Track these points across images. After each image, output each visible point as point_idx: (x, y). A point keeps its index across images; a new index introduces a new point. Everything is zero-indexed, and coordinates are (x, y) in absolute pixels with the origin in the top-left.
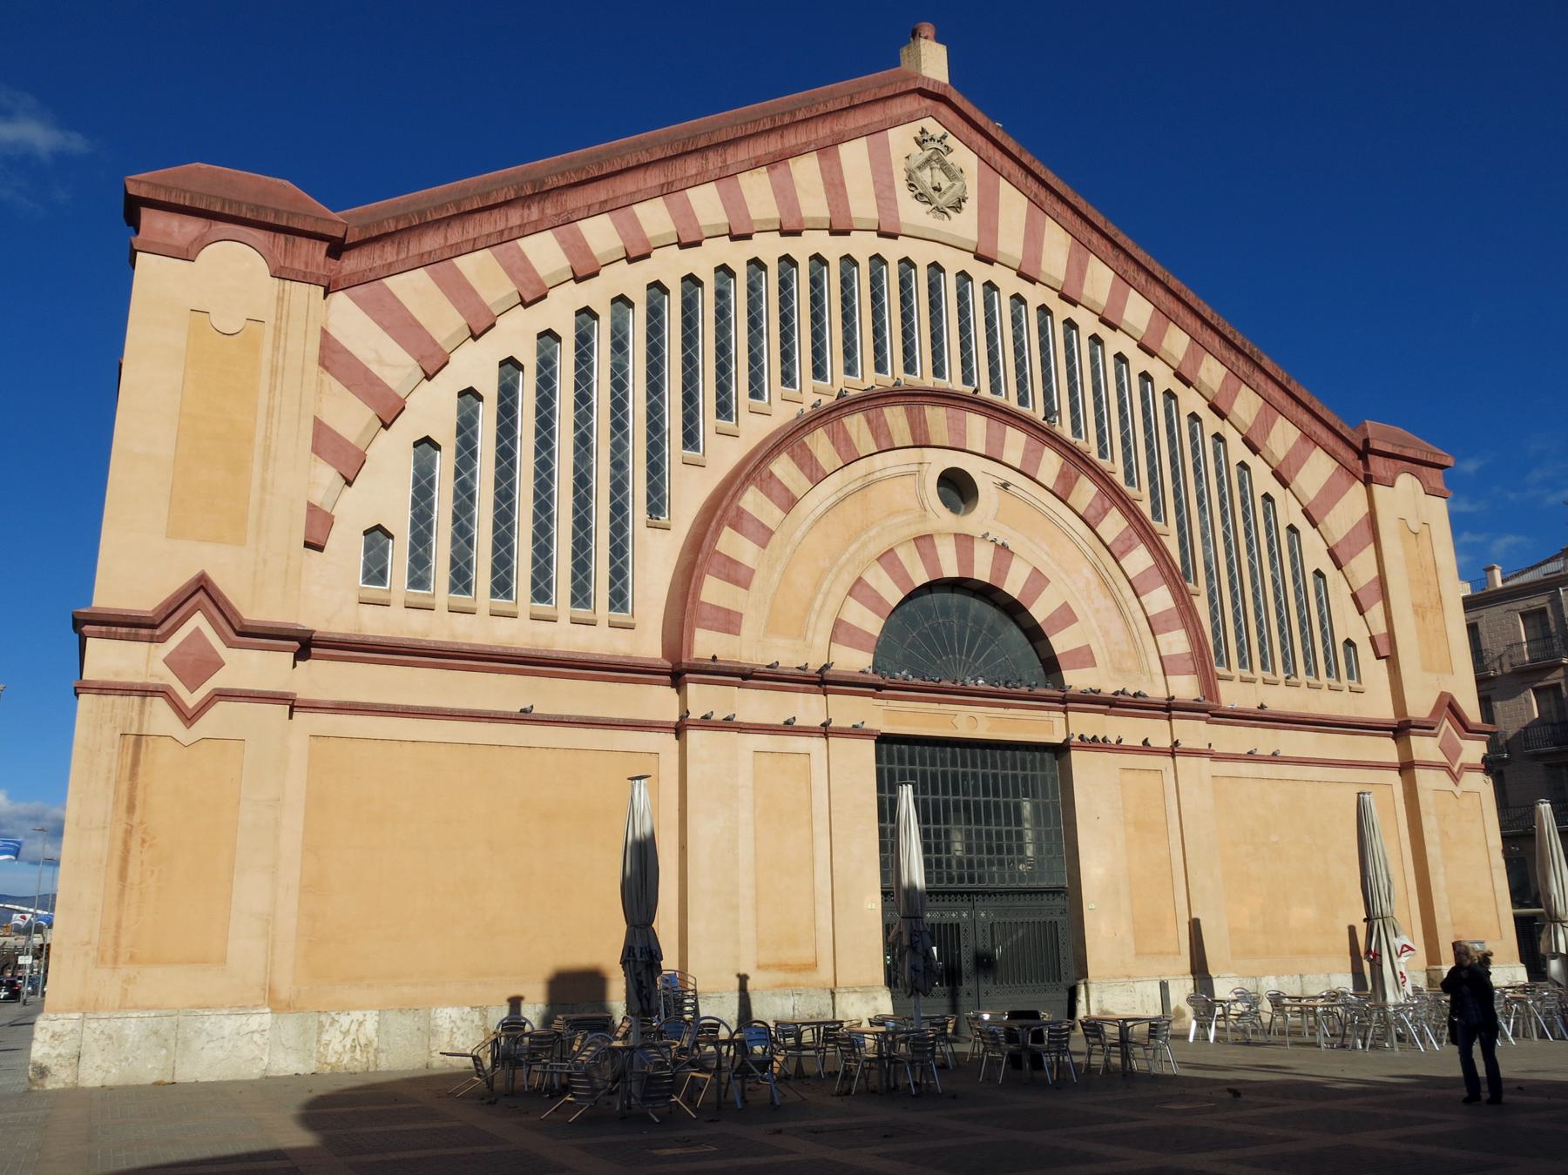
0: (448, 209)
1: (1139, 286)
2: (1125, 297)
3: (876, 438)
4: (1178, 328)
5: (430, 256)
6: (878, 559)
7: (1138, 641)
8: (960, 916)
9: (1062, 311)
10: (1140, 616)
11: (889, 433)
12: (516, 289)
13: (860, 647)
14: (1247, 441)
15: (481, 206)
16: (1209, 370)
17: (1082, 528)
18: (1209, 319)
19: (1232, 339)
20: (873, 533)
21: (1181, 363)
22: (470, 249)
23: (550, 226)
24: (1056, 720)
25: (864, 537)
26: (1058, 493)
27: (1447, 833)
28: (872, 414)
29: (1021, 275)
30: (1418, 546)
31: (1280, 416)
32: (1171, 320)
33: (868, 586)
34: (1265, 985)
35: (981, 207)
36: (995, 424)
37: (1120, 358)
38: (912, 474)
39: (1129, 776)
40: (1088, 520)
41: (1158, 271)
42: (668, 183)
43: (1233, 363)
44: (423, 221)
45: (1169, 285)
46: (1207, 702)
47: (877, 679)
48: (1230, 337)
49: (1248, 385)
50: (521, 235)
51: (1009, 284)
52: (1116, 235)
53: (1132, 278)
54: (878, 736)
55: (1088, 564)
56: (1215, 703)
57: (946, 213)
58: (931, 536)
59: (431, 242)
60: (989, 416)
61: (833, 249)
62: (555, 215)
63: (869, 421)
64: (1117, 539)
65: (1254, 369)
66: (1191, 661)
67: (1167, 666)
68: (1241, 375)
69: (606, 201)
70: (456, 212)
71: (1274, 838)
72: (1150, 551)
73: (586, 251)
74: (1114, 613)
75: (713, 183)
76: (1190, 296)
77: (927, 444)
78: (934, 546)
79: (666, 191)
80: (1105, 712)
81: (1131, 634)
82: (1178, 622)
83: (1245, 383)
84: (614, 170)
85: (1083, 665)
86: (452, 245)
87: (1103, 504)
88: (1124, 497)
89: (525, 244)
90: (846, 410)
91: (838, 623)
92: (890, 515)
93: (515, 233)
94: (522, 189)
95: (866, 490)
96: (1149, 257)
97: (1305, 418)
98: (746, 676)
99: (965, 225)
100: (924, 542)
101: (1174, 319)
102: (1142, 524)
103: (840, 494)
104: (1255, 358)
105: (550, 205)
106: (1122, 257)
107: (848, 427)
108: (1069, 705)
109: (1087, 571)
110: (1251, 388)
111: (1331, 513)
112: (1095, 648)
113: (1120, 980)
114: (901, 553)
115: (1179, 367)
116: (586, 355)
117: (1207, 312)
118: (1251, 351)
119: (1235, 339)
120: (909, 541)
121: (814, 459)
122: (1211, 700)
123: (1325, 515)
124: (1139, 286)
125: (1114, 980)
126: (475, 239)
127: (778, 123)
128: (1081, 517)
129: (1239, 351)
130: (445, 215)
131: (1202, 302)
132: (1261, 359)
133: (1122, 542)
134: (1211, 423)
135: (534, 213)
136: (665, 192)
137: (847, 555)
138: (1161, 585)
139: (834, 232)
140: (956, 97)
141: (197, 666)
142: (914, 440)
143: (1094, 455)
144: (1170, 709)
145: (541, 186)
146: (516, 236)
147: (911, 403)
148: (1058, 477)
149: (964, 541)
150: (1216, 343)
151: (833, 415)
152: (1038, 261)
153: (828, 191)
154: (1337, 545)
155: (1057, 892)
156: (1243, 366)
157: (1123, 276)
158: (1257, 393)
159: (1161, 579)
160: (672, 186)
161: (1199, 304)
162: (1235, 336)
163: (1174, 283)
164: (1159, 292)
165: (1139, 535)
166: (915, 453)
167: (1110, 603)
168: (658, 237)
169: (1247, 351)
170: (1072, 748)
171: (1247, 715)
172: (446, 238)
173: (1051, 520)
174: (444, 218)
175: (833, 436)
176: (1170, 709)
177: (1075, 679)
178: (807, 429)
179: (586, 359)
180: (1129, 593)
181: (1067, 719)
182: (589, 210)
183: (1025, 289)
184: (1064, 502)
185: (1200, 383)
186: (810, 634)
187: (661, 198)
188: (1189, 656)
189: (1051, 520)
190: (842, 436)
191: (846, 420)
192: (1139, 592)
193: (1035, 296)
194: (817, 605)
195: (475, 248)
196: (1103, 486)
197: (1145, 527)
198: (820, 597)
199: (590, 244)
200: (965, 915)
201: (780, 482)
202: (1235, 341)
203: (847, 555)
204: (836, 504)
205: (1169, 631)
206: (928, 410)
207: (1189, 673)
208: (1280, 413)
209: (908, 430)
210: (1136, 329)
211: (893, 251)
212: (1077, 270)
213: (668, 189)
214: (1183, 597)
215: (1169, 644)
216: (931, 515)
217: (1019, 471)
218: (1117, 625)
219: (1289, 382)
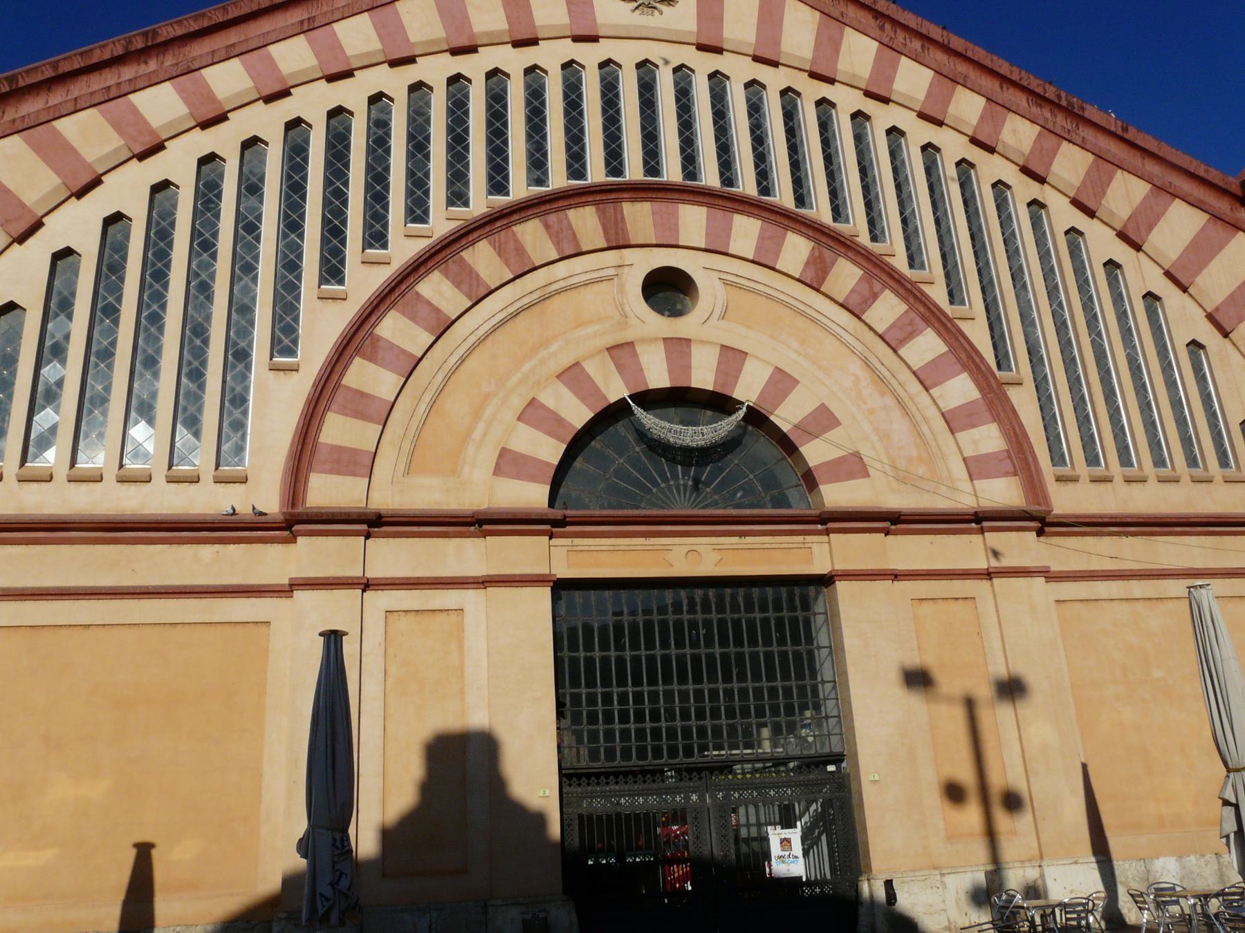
0: (43, 72)
1: (910, 51)
2: (895, 67)
3: (557, 244)
4: (968, 92)
5: (23, 121)
6: (558, 377)
7: (932, 443)
8: (687, 798)
9: (811, 91)
10: (932, 412)
11: (574, 234)
12: (123, 142)
13: (533, 479)
14: (1076, 203)
15: (83, 65)
16: (1014, 131)
17: (844, 317)
18: (1009, 76)
19: (1042, 93)
20: (554, 347)
21: (976, 128)
22: (72, 109)
23: (166, 78)
24: (816, 548)
25: (543, 354)
26: (808, 281)
28: (552, 218)
29: (756, 59)
31: (1119, 171)
32: (958, 83)
33: (543, 407)
34: (1159, 869)
36: (719, 214)
37: (894, 133)
39: (927, 608)
40: (850, 308)
41: (935, 32)
42: (309, 19)
43: (1046, 119)
44: (14, 87)
45: (951, 46)
46: (1033, 508)
47: (557, 513)
48: (1039, 90)
49: (1070, 141)
50: (133, 89)
51: (739, 70)
53: (900, 45)
54: (554, 582)
55: (856, 358)
56: (1043, 508)
57: (655, 8)
58: (631, 344)
59: (31, 107)
60: (709, 205)
61: (514, 61)
62: (173, 65)
63: (547, 227)
64: (892, 326)
65: (1077, 125)
67: (977, 468)
68: (1058, 131)
69: (233, 45)
70: (53, 75)
71: (1158, 674)
72: (940, 335)
73: (210, 95)
74: (896, 413)
75: (366, 13)
76: (979, 54)
77: (626, 243)
78: (635, 355)
79: (306, 28)
80: (887, 533)
81: (920, 435)
82: (987, 415)
83: (1066, 139)
84: (242, 13)
85: (850, 476)
86: (50, 107)
87: (871, 288)
88: (897, 276)
89: (139, 99)
90: (516, 217)
91: (504, 452)
92: (579, 325)
93: (125, 88)
95: (548, 301)
96: (920, 19)
97: (1152, 168)
100: (622, 353)
101: (961, 81)
102: (925, 305)
103: (511, 310)
104: (1076, 111)
105: (170, 58)
106: (888, 26)
107: (519, 235)
108: (831, 525)
109: (856, 367)
110: (1074, 144)
111: (1205, 272)
112: (866, 453)
113: (917, 874)
114: (591, 368)
115: (975, 132)
116: (213, 202)
117: (1004, 67)
118: (1069, 103)
119: (1045, 93)
120: (601, 351)
121: (474, 275)
122: (1039, 504)
123: (1196, 276)
124: (910, 51)
125: (912, 874)
126: (76, 99)
128: (842, 305)
129: (1055, 105)
130: (40, 77)
131: (995, 58)
132: (1083, 109)
133: (901, 329)
134: (1023, 190)
135: (152, 65)
136: (306, 28)
137: (519, 375)
138: (959, 374)
139: (517, 44)
142: (607, 240)
143: (864, 239)
144: (979, 520)
145: (153, 38)
146: (126, 91)
148: (807, 263)
149: (678, 348)
150: (1021, 100)
151: (498, 224)
152: (777, 43)
154: (1217, 309)
155: (837, 759)
156: (1061, 122)
157: (890, 45)
158: (1083, 148)
159: (958, 367)
160: (314, 22)
161: (992, 61)
163: (957, 43)
164: (939, 56)
165: (924, 319)
166: (612, 257)
167: (889, 401)
168: (292, 75)
169: (1064, 103)
170: (836, 578)
171: (1100, 520)
172: (47, 102)
173: (802, 314)
175: (500, 247)
176: (979, 520)
177: (835, 495)
178: (464, 242)
179: (212, 206)
180: (914, 386)
181: (829, 543)
182: (213, 56)
183: (763, 73)
184: (818, 290)
185: (1004, 146)
186: (467, 468)
187: (302, 35)
188: (1006, 454)
189: (802, 314)
190: (511, 245)
191: (517, 229)
192: (927, 383)
193: (774, 80)
194: (477, 435)
195: (78, 107)
196: (870, 267)
197: (929, 308)
198: (481, 426)
199: (213, 89)
200: (694, 797)
201: (429, 303)
202: (1047, 95)
203: (519, 375)
204: (503, 322)
205: (973, 426)
206: (627, 208)
207: (1006, 474)
208: (1120, 168)
209: (600, 230)
210: (911, 98)
211: (589, 56)
212: (828, 45)
213: (309, 25)
214: (989, 384)
215: (975, 442)
216: (634, 321)
217: (753, 262)
218: (899, 427)
219: (1125, 130)
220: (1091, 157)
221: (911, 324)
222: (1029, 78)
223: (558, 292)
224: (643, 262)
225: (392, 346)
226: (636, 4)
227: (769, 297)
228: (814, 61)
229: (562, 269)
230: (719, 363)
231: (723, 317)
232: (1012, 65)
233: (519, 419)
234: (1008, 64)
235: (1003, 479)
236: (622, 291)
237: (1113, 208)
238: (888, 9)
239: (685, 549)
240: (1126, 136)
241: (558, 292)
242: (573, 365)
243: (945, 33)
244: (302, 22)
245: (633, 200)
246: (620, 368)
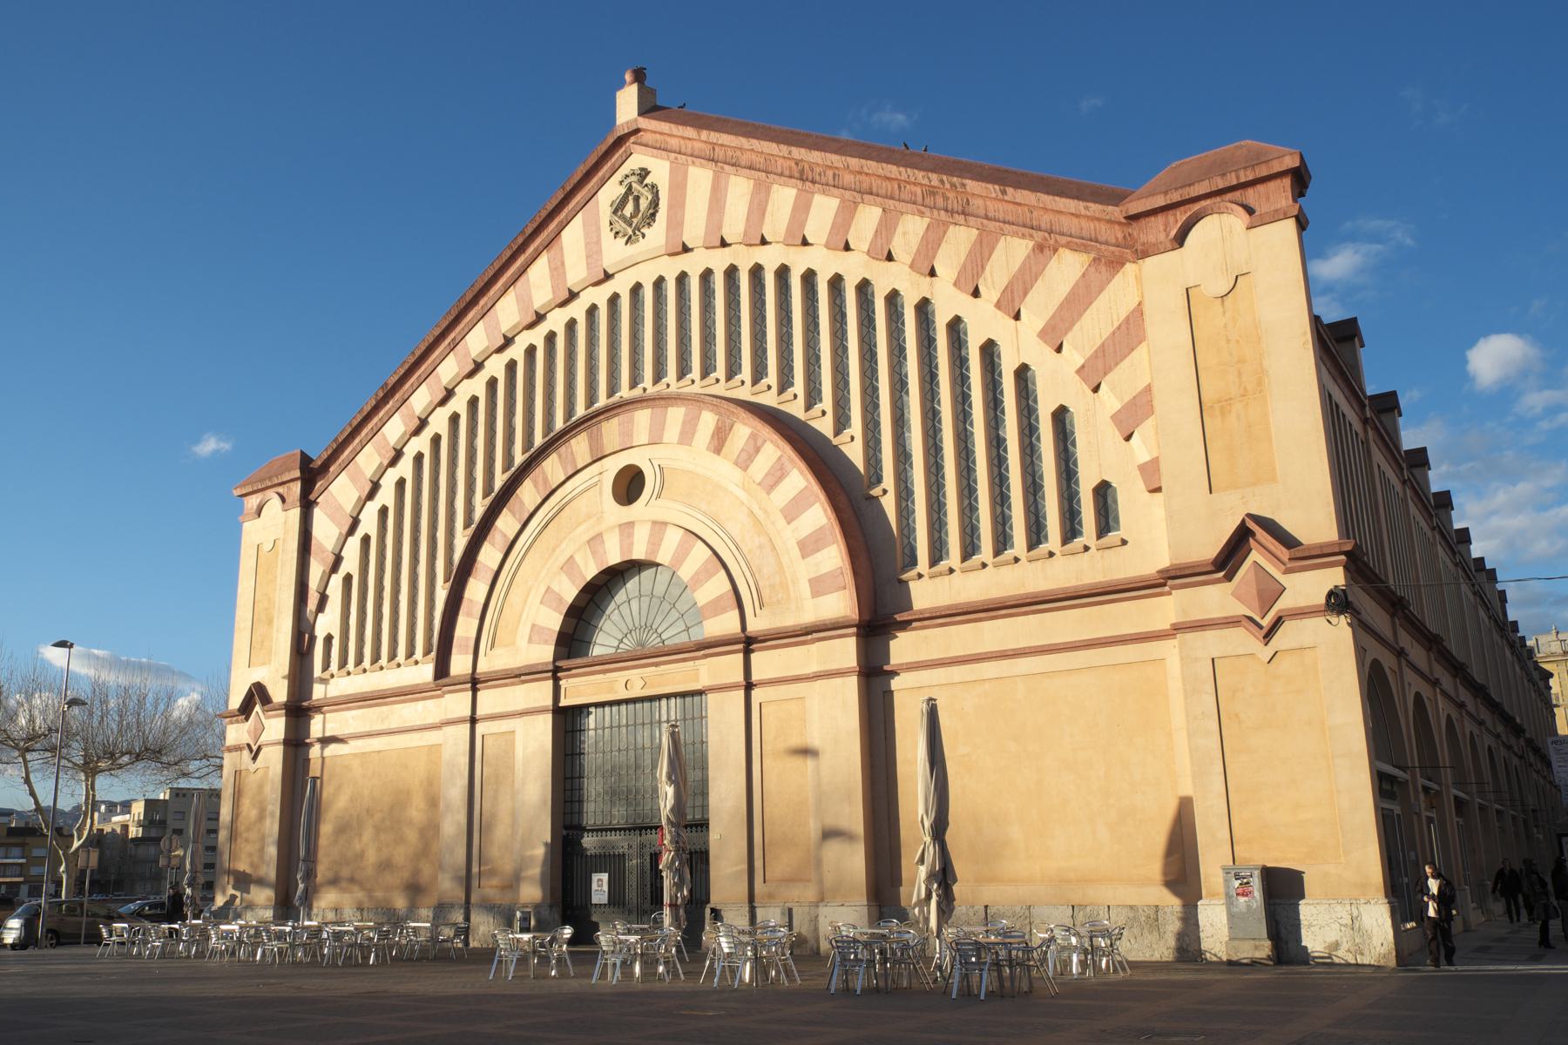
20: (564, 545)
27: (1237, 715)
30: (1224, 313)
35: (670, 207)
36: (658, 411)
38: (595, 485)
49: (956, 224)
52: (790, 153)
66: (841, 576)
67: (819, 586)
91: (533, 626)
94: (377, 395)
96: (823, 153)
99: (656, 235)
111: (1076, 327)
127: (515, 248)
131: (884, 165)
133: (773, 475)
136: (452, 346)
140: (644, 123)
147: (589, 427)
153: (552, 277)
161: (883, 169)
162: (929, 178)
174: (349, 435)
201: (501, 531)
204: (540, 533)
221: (781, 469)
222: (914, 173)
224: (613, 466)
226: (626, 238)
228: (745, 234)
230: (650, 535)
231: (659, 496)
232: (898, 166)
233: (541, 603)
234: (895, 167)
235: (835, 594)
238: (800, 154)
242: (568, 560)
243: (843, 158)
244: (449, 344)
245: (608, 419)
246: (594, 553)
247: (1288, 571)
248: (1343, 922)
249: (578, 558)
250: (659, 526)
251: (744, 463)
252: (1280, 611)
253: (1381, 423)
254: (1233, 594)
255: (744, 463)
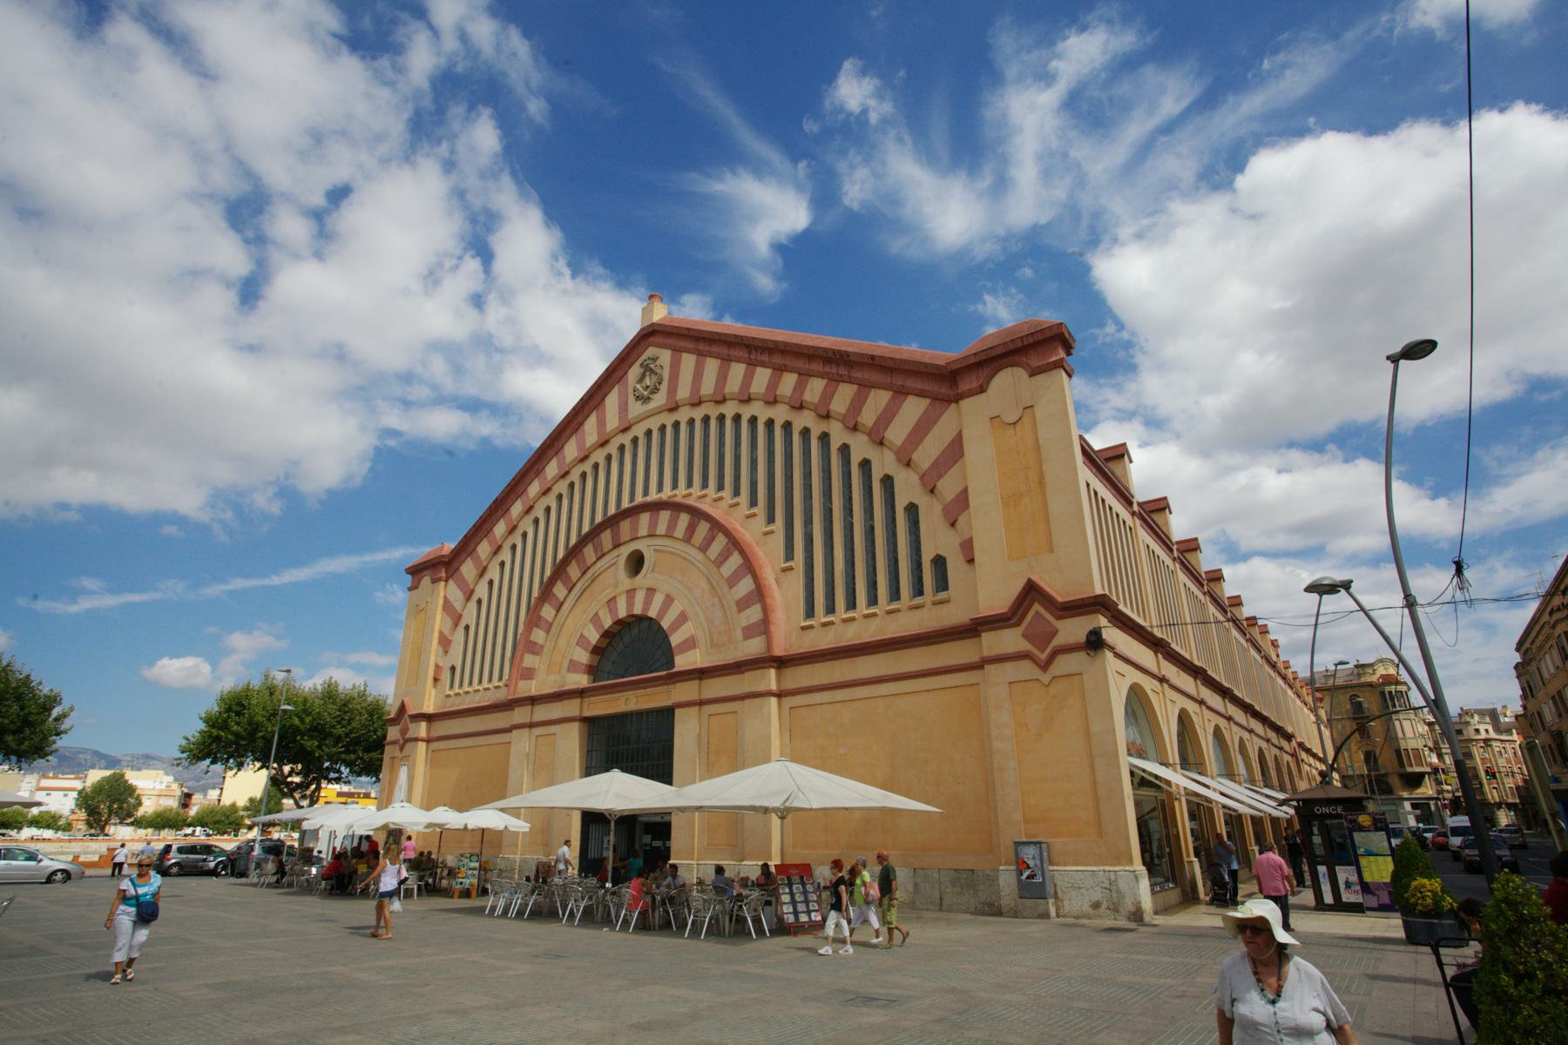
27: (1026, 725)
60: (651, 511)
85: (689, 649)
91: (571, 661)
98: (533, 701)
99: (659, 400)
109: (703, 584)
111: (920, 448)
141: (1042, 637)
148: (687, 529)
177: (682, 662)
208: (873, 387)
220: (856, 386)
221: (729, 548)
223: (600, 574)
224: (625, 551)
225: (545, 619)
227: (672, 553)
229: (599, 565)
231: (653, 570)
233: (577, 644)
236: (617, 570)
237: (864, 422)
239: (624, 699)
240: (875, 363)
241: (600, 574)
247: (1059, 618)
248: (1104, 885)
249: (601, 614)
250: (651, 591)
251: (704, 549)
252: (1054, 647)
253: (1152, 520)
254: (1023, 636)
255: (704, 549)
